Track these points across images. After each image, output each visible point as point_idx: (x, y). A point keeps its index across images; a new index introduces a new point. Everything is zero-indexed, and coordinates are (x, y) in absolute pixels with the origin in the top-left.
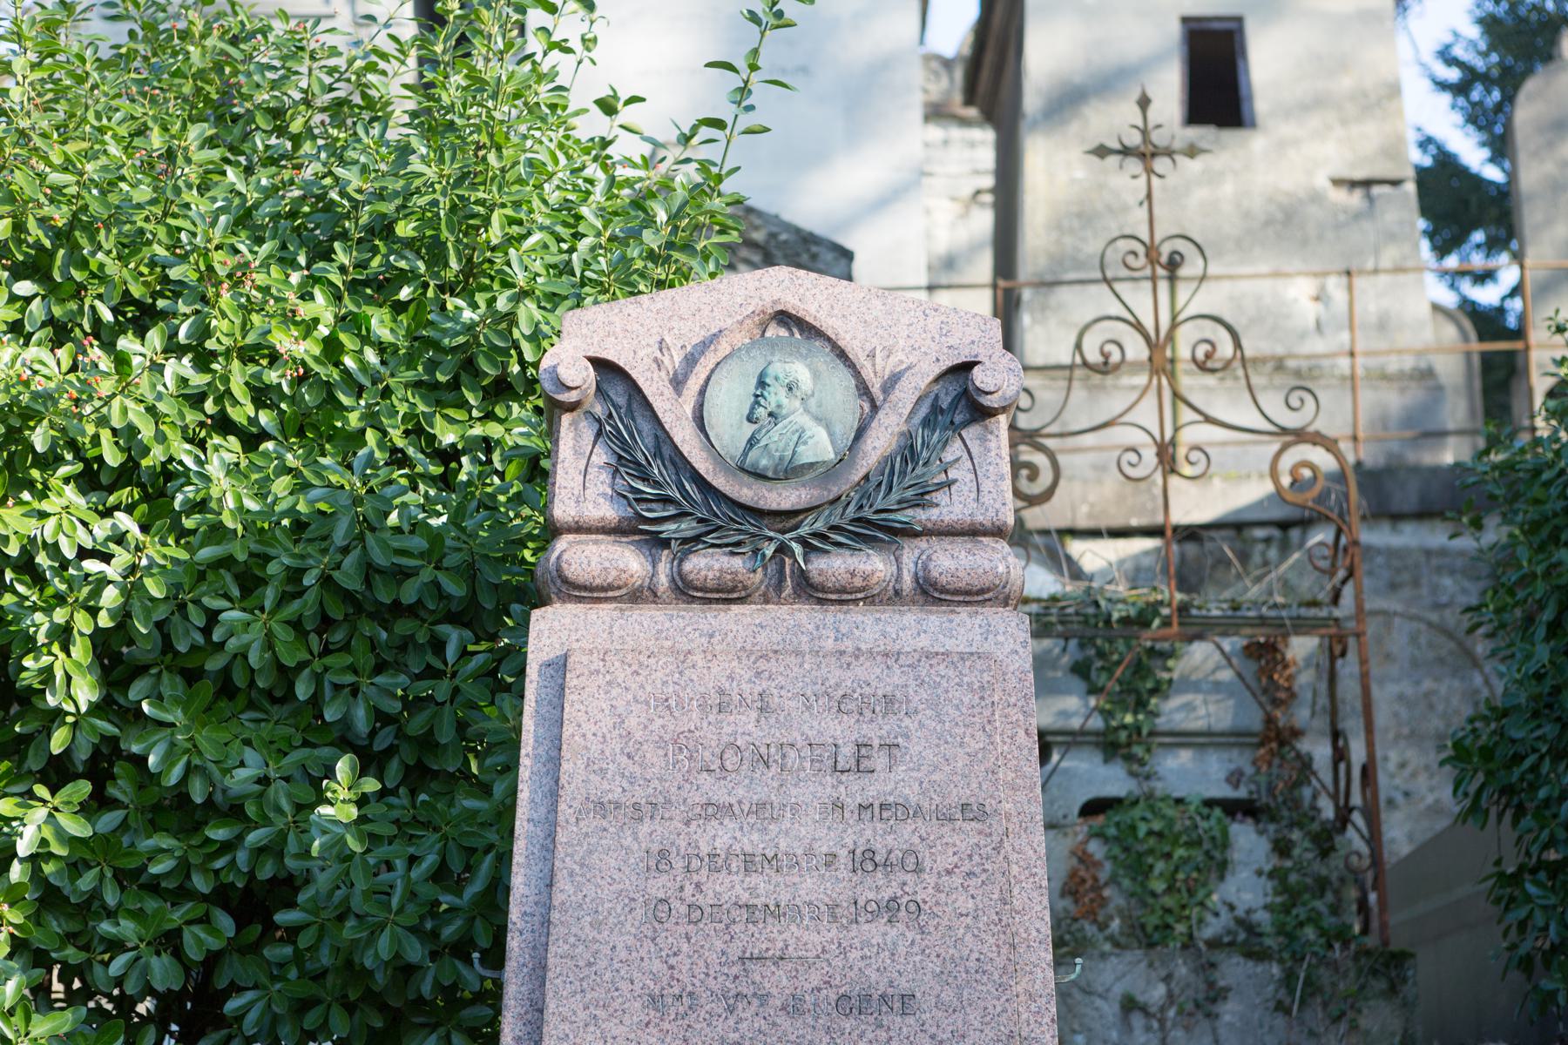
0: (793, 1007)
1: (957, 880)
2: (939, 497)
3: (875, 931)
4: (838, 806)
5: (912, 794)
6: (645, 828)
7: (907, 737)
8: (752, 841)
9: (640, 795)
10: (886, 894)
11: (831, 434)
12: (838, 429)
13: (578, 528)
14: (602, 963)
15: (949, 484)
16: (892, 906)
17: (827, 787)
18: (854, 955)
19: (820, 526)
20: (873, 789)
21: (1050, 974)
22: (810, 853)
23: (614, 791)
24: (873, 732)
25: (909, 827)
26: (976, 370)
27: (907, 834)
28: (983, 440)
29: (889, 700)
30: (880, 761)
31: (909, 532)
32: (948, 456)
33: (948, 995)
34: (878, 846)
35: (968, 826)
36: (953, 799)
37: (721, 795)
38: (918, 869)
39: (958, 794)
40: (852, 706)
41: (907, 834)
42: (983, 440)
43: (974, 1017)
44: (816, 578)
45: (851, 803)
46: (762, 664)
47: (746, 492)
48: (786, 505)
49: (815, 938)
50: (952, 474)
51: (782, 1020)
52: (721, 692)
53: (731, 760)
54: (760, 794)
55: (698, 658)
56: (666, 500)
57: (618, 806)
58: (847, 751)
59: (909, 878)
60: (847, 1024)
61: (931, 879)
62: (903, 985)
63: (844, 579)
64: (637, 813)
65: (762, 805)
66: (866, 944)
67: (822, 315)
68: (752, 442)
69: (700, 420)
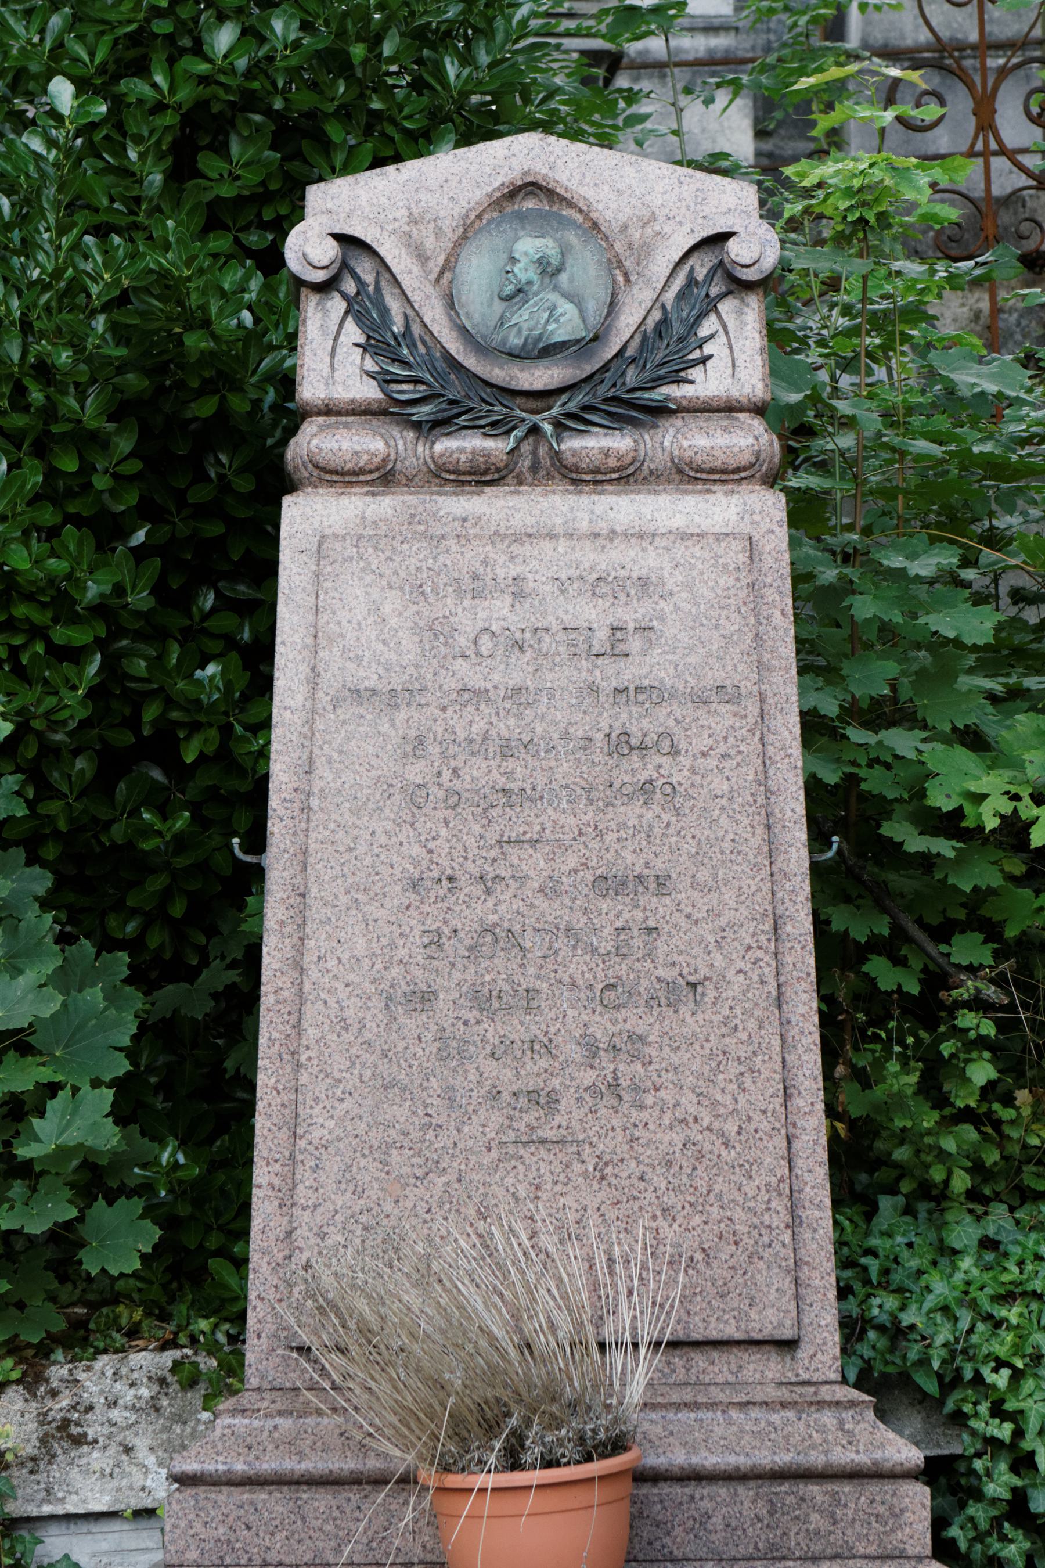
0: (551, 889)
1: (712, 762)
2: (695, 373)
3: (632, 813)
4: (593, 689)
5: (665, 675)
6: (402, 715)
7: (662, 619)
8: (507, 727)
9: (397, 682)
10: (643, 776)
11: (582, 312)
12: (591, 306)
13: (328, 410)
14: (362, 849)
15: (704, 360)
16: (646, 788)
17: (582, 672)
18: (610, 837)
19: (572, 406)
20: (630, 673)
21: (805, 853)
22: (565, 736)
23: (369, 677)
24: (628, 615)
25: (663, 711)
26: (732, 244)
27: (663, 717)
28: (740, 313)
29: (644, 583)
30: (635, 644)
31: (660, 411)
32: (703, 332)
33: (703, 875)
34: (633, 729)
35: (723, 709)
36: (709, 682)
37: (476, 682)
38: (674, 751)
39: (714, 676)
40: (605, 589)
41: (663, 717)
42: (740, 313)
43: (729, 896)
44: (570, 460)
45: (608, 687)
46: (516, 549)
47: (498, 373)
48: (538, 386)
49: (572, 821)
50: (708, 349)
51: (541, 902)
52: (475, 577)
53: (486, 644)
54: (516, 679)
55: (452, 543)
56: (416, 381)
57: (374, 692)
58: (602, 635)
59: (665, 761)
60: (605, 905)
61: (685, 761)
62: (659, 866)
63: (598, 459)
64: (393, 699)
65: (518, 690)
66: (622, 826)
67: (573, 185)
68: (502, 321)
69: (450, 302)
